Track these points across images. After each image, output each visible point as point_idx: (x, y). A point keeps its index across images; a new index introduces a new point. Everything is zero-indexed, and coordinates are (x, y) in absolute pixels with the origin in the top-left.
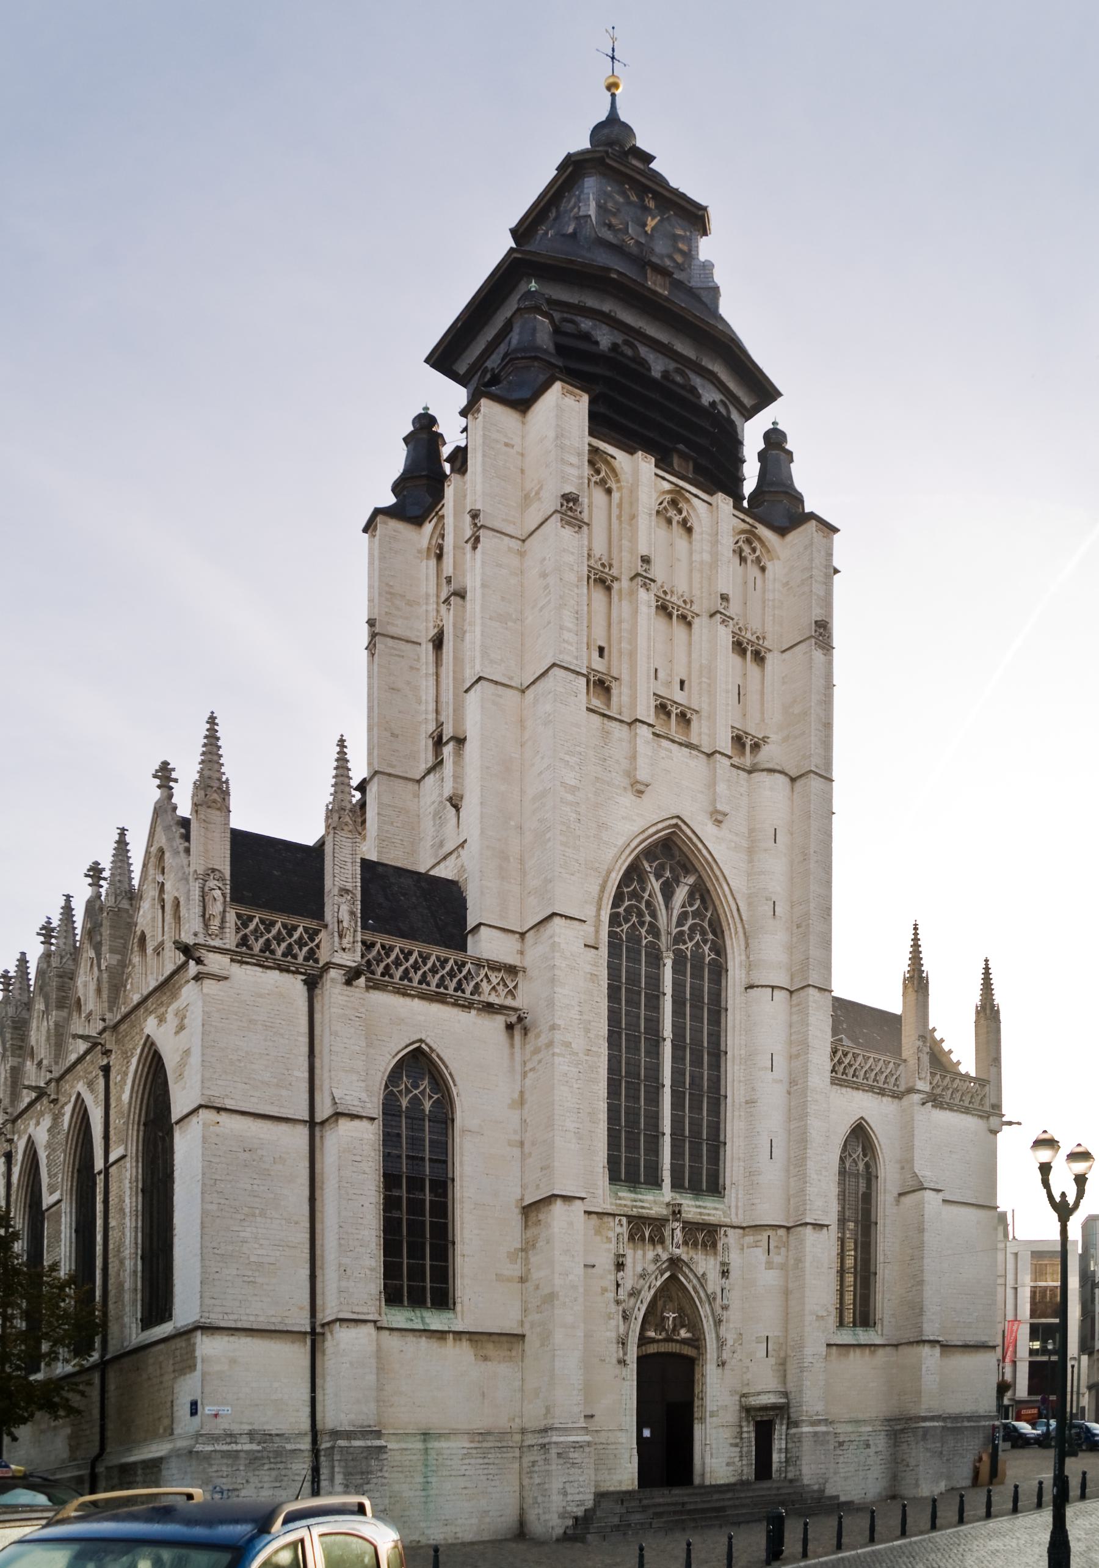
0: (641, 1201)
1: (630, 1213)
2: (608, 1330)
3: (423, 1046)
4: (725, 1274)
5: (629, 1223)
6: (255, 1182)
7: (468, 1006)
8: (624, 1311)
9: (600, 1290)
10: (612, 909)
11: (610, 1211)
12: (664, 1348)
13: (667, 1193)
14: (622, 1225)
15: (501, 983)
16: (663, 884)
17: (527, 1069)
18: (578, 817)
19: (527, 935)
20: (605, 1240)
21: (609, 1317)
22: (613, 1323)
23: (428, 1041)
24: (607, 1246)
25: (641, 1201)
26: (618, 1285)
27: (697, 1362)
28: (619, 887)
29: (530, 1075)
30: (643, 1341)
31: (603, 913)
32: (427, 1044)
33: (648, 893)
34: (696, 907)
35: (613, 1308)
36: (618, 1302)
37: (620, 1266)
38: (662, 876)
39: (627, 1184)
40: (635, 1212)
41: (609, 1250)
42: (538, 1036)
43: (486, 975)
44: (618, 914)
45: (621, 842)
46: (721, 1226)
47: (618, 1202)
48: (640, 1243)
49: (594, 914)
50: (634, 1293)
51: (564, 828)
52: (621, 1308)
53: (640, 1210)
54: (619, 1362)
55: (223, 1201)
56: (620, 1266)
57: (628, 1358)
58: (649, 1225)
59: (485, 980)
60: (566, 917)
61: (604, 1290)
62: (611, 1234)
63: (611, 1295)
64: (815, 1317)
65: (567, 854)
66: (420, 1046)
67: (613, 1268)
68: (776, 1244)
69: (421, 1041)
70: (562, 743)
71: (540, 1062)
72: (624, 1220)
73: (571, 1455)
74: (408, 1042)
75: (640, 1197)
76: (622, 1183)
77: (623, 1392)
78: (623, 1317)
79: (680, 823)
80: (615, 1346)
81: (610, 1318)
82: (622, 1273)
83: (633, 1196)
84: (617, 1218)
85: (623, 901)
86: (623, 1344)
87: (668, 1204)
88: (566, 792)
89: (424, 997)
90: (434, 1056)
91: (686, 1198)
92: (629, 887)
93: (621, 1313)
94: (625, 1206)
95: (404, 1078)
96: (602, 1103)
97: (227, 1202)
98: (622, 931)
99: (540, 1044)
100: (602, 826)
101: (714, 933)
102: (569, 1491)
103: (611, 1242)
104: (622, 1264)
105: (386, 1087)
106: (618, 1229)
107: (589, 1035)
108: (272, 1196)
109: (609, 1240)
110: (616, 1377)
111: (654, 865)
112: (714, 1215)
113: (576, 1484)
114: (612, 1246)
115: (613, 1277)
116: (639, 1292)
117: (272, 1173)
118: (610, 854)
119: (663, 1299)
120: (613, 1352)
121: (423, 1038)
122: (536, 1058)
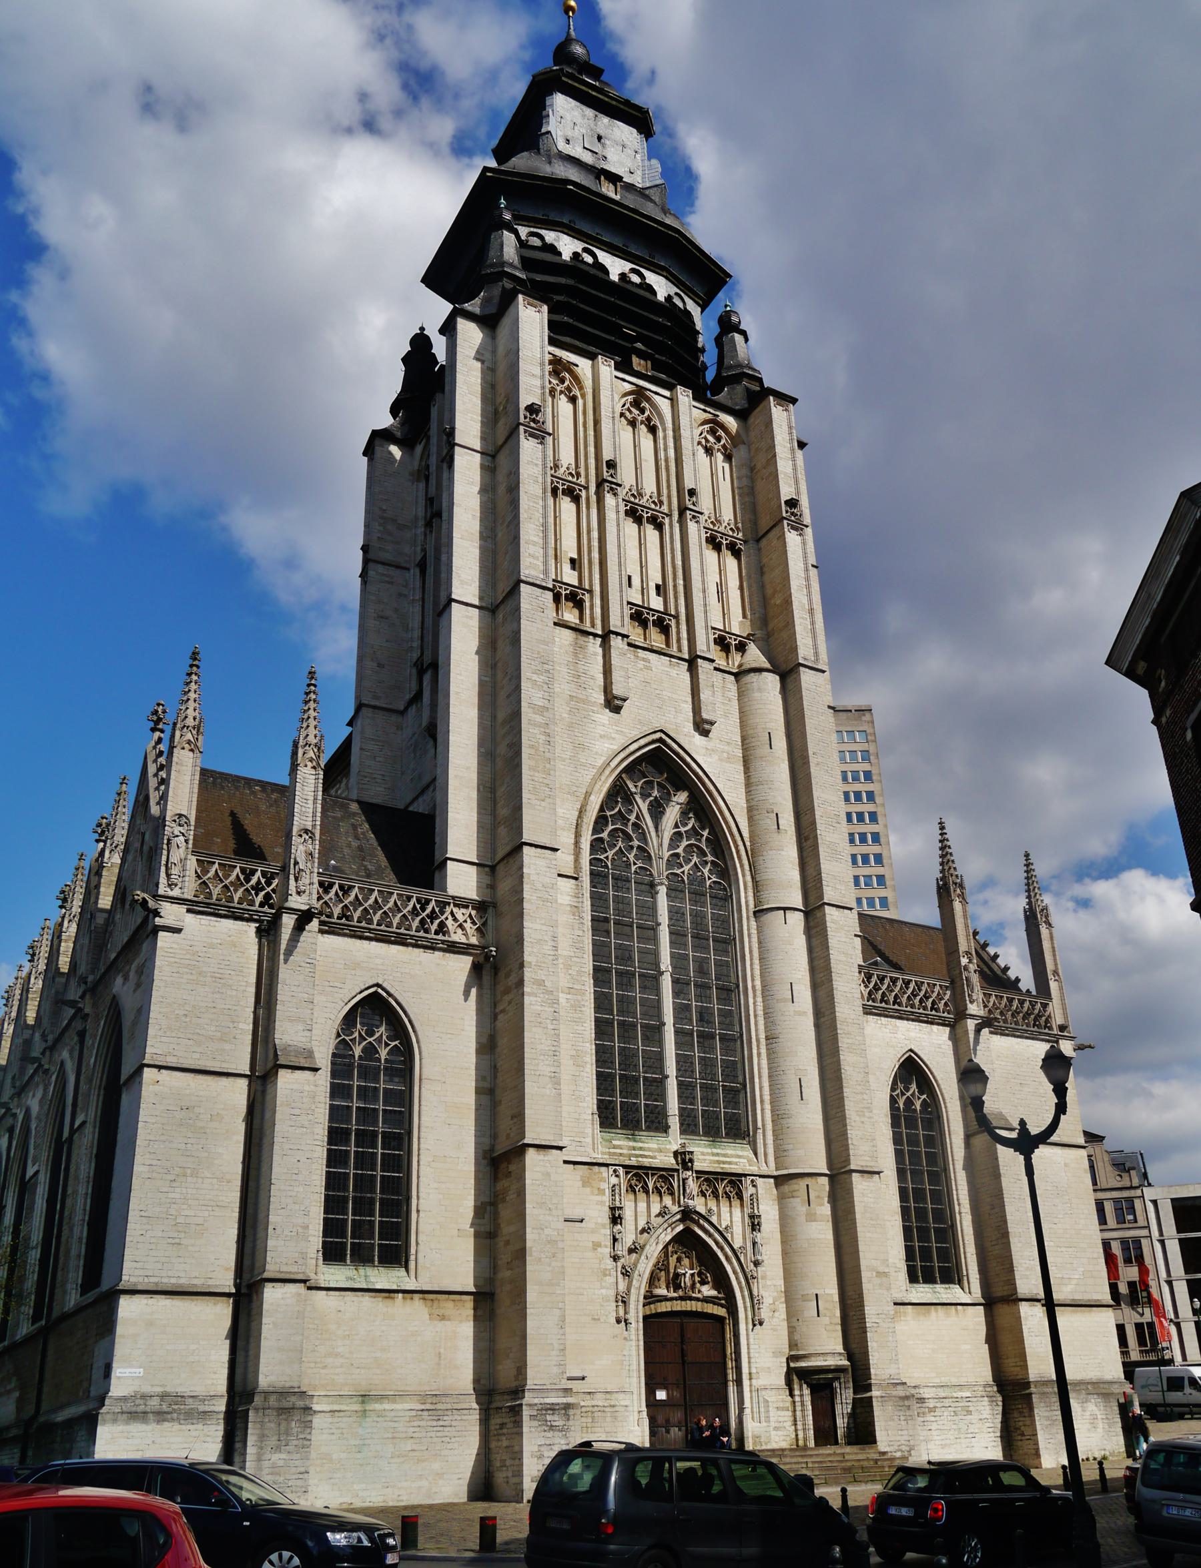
0: (641, 1149)
1: (627, 1163)
2: (602, 1287)
3: (380, 991)
5: (627, 1173)
6: (189, 1141)
7: (432, 948)
8: (623, 1267)
10: (592, 835)
11: (601, 1161)
12: (679, 1306)
13: (674, 1140)
14: (617, 1176)
15: (468, 920)
16: (651, 804)
17: (497, 1011)
18: (548, 739)
19: (498, 868)
20: (596, 1192)
21: (605, 1273)
22: (610, 1280)
23: (385, 985)
24: (599, 1198)
25: (641, 1149)
26: (615, 1240)
28: (601, 809)
29: (500, 1017)
30: (650, 1298)
31: (583, 840)
32: (384, 989)
33: (634, 815)
34: (690, 826)
36: (615, 1258)
37: (616, 1219)
38: (650, 795)
39: (624, 1132)
40: (633, 1161)
41: (602, 1203)
42: (508, 975)
43: (452, 913)
44: (601, 840)
45: (600, 762)
47: (612, 1150)
48: (642, 1196)
49: (573, 841)
51: (533, 751)
52: (619, 1264)
53: (640, 1159)
54: (618, 1321)
55: (155, 1162)
56: (616, 1219)
57: (631, 1317)
58: (653, 1175)
59: (450, 917)
60: (537, 846)
61: (596, 1245)
62: (605, 1186)
63: (607, 1250)
65: (536, 779)
66: (376, 992)
67: (607, 1221)
70: (529, 661)
71: (510, 1003)
72: (621, 1171)
74: (363, 987)
75: (641, 1145)
76: (618, 1131)
77: (625, 1353)
78: (622, 1273)
79: (664, 737)
80: (615, 1304)
81: (605, 1275)
82: (619, 1227)
83: (631, 1144)
84: (611, 1169)
85: (607, 825)
86: (624, 1302)
87: (676, 1154)
88: (534, 713)
90: (390, 1000)
91: (699, 1145)
92: (613, 809)
93: (619, 1269)
94: (621, 1154)
95: (358, 1026)
96: (588, 1045)
97: (159, 1163)
98: (607, 858)
99: (510, 983)
100: (580, 747)
101: (715, 854)
103: (604, 1194)
104: (620, 1217)
105: (338, 1035)
106: (614, 1180)
107: (570, 972)
108: (206, 1154)
109: (601, 1192)
111: (640, 784)
114: (606, 1198)
115: (608, 1232)
116: (642, 1248)
117: (208, 1131)
118: (588, 776)
119: (675, 1256)
120: (611, 1311)
121: (380, 983)
122: (507, 998)
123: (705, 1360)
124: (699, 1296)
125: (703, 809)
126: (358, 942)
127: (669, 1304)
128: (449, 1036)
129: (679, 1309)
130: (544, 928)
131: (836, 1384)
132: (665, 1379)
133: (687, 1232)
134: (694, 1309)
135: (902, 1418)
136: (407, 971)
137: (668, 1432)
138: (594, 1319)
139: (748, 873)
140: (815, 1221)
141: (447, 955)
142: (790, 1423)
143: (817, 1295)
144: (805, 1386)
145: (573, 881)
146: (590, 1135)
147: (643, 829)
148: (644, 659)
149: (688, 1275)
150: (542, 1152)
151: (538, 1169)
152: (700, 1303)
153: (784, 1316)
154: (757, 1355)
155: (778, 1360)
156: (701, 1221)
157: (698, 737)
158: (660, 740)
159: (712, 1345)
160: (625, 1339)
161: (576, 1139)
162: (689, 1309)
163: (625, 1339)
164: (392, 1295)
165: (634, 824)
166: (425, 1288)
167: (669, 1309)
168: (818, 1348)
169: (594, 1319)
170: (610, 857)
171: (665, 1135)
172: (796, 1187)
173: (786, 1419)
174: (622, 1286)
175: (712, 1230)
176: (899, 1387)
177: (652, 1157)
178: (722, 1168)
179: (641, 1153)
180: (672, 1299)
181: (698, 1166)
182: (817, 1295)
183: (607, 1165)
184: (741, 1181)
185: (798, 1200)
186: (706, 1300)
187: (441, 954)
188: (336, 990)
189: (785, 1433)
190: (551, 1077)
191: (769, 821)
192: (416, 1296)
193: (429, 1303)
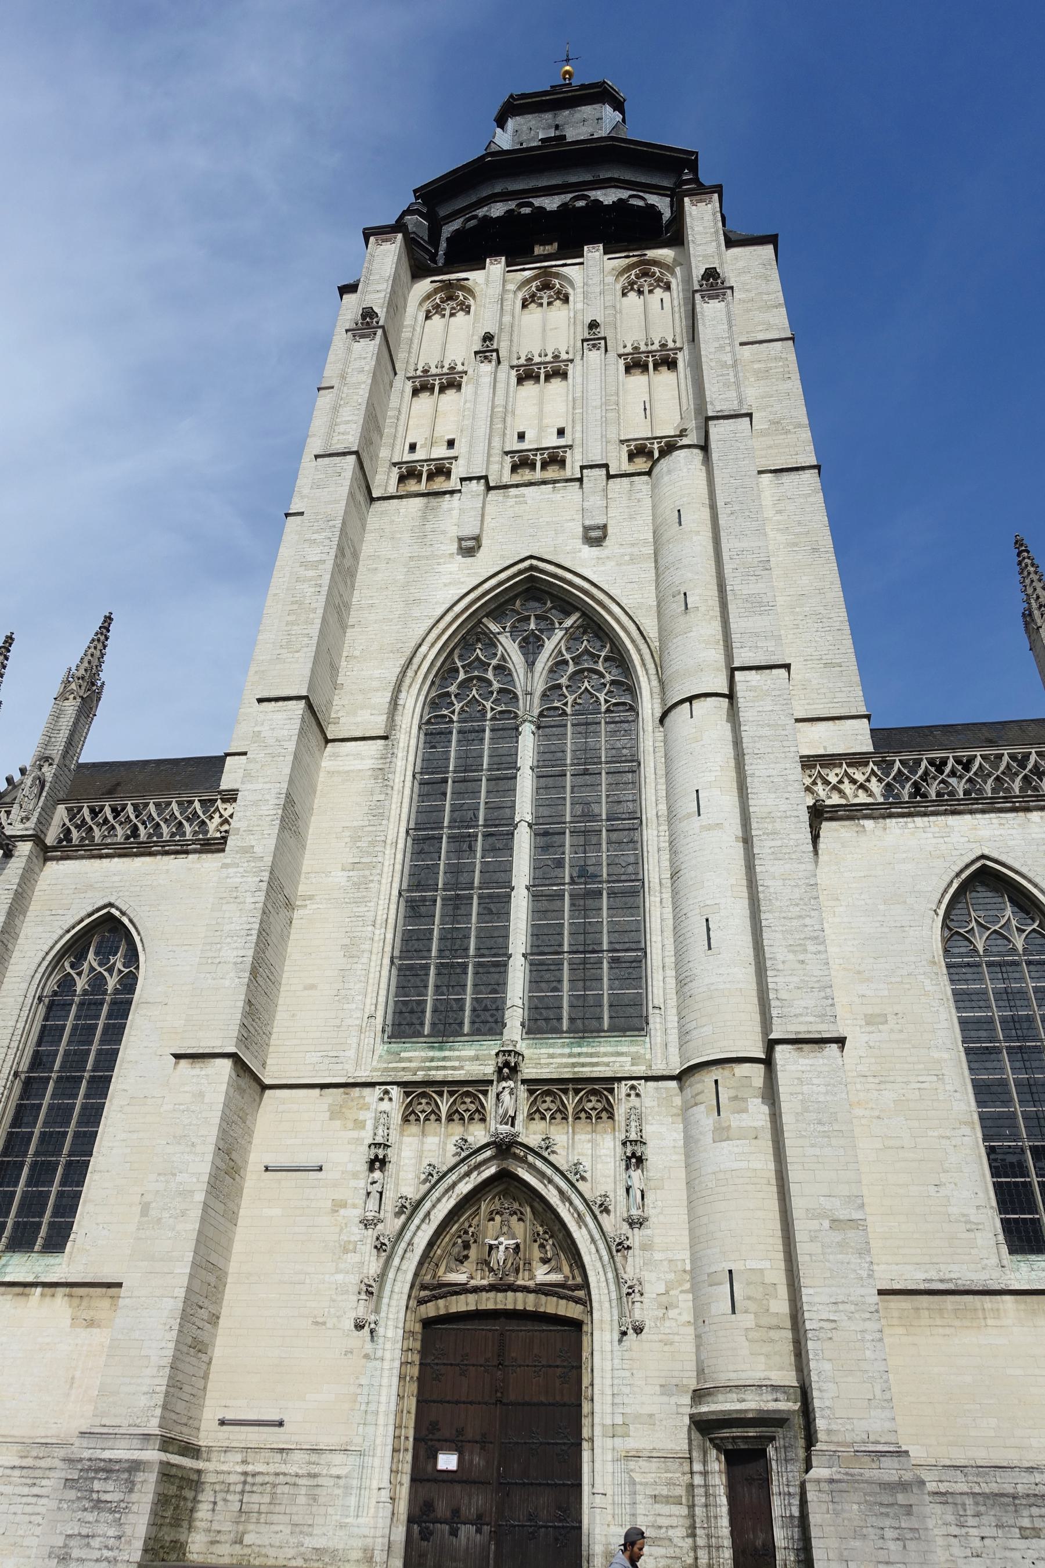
1: (408, 1077)
2: (338, 1271)
3: (113, 911)
4: (635, 1160)
9: (329, 1204)
20: (350, 1125)
21: (347, 1248)
23: (117, 904)
24: (354, 1134)
27: (585, 1328)
32: (117, 909)
35: (356, 1231)
37: (378, 1163)
46: (620, 1079)
50: (409, 1209)
54: (359, 1327)
56: (378, 1163)
64: (826, 1224)
68: (732, 1093)
69: (111, 905)
72: (395, 1091)
73: (97, 1485)
75: (457, 1053)
81: (346, 1251)
89: (123, 852)
102: (76, 1553)
103: (363, 1127)
107: (359, 844)
109: (360, 1125)
110: (349, 1352)
112: (607, 1065)
113: (96, 1543)
115: (362, 1184)
121: (112, 901)
123: (543, 1399)
124: (531, 1284)
125: (600, 627)
126: (96, 863)
127: (472, 1298)
128: (186, 948)
129: (490, 1306)
130: (268, 786)
131: (771, 1451)
132: (460, 1432)
133: (504, 1177)
134: (520, 1307)
135: (889, 1534)
136: (149, 883)
137: (454, 1533)
138: (316, 1323)
139: (654, 678)
140: (728, 1139)
141: (204, 856)
142: (681, 1532)
143: (730, 1272)
144: (713, 1453)
145: (382, 742)
146: (355, 1045)
147: (510, 670)
148: (516, 496)
149: (502, 1248)
150: (199, 1064)
151: (187, 1088)
152: (531, 1297)
153: (688, 1316)
154: (626, 1390)
155: (673, 1400)
156: (530, 1159)
157: (588, 552)
158: (532, 568)
159: (559, 1371)
160: (367, 1356)
161: (331, 1054)
162: (510, 1306)
163: (367, 1356)
164: (27, 1290)
165: (495, 668)
166: (72, 1279)
167: (472, 1307)
168: (733, 1376)
169: (316, 1323)
170: (457, 711)
171: (498, 1037)
172: (699, 1087)
173: (674, 1521)
174: (373, 1267)
175: (549, 1171)
176: (886, 1462)
177: (454, 1068)
178: (575, 1073)
179: (441, 1064)
180: (476, 1290)
181: (528, 1071)
182: (730, 1272)
183: (372, 1085)
184: (611, 1091)
185: (702, 1108)
186: (543, 1290)
187: (196, 856)
188: (58, 917)
189: (670, 1552)
190: (236, 963)
191: (674, 606)
192: (61, 1291)
193: (76, 1301)
